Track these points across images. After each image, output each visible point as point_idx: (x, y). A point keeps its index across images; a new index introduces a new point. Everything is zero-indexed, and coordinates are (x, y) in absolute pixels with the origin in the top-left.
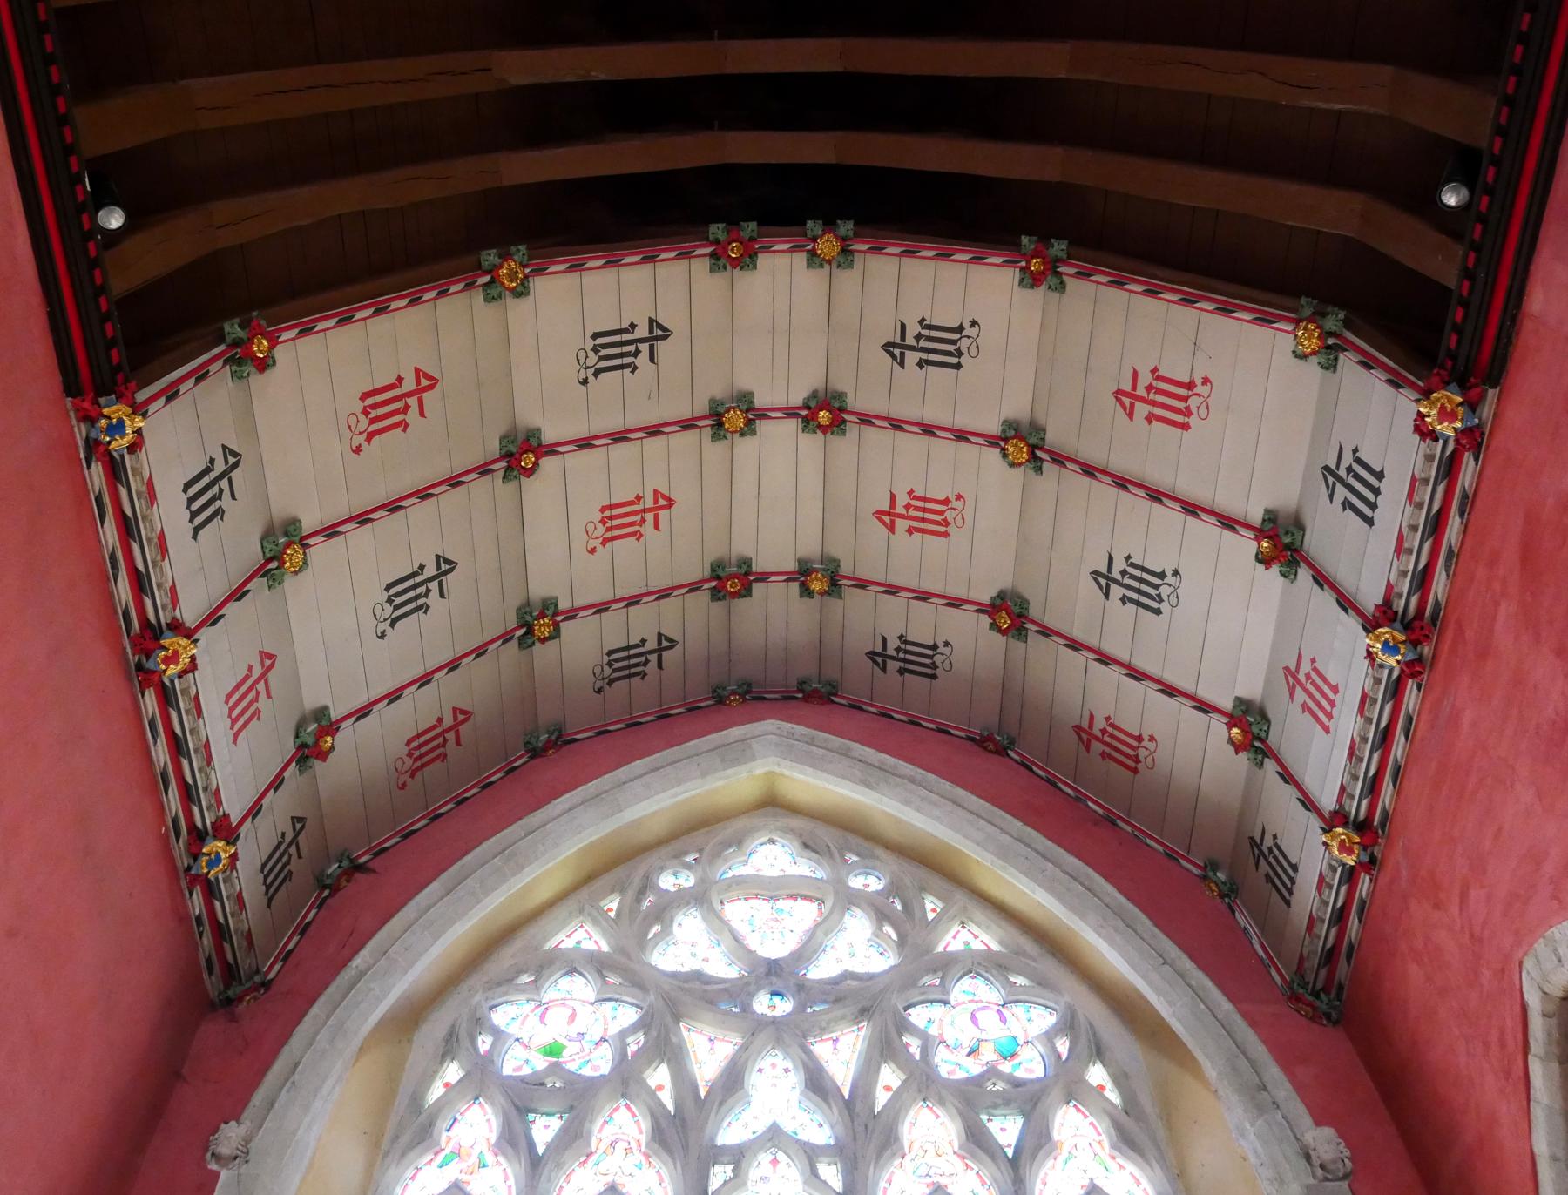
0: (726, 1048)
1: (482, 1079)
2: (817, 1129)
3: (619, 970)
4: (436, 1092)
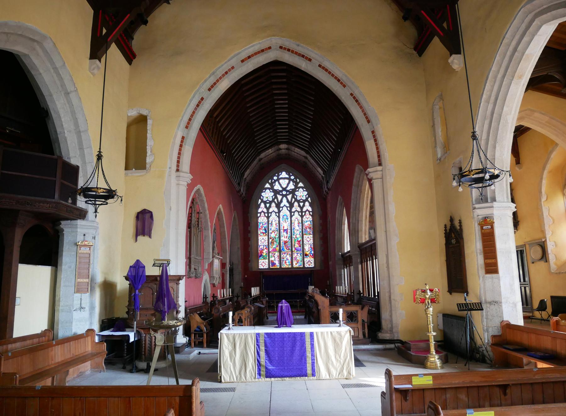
0: (281, 197)
1: (262, 201)
2: (288, 205)
3: (272, 188)
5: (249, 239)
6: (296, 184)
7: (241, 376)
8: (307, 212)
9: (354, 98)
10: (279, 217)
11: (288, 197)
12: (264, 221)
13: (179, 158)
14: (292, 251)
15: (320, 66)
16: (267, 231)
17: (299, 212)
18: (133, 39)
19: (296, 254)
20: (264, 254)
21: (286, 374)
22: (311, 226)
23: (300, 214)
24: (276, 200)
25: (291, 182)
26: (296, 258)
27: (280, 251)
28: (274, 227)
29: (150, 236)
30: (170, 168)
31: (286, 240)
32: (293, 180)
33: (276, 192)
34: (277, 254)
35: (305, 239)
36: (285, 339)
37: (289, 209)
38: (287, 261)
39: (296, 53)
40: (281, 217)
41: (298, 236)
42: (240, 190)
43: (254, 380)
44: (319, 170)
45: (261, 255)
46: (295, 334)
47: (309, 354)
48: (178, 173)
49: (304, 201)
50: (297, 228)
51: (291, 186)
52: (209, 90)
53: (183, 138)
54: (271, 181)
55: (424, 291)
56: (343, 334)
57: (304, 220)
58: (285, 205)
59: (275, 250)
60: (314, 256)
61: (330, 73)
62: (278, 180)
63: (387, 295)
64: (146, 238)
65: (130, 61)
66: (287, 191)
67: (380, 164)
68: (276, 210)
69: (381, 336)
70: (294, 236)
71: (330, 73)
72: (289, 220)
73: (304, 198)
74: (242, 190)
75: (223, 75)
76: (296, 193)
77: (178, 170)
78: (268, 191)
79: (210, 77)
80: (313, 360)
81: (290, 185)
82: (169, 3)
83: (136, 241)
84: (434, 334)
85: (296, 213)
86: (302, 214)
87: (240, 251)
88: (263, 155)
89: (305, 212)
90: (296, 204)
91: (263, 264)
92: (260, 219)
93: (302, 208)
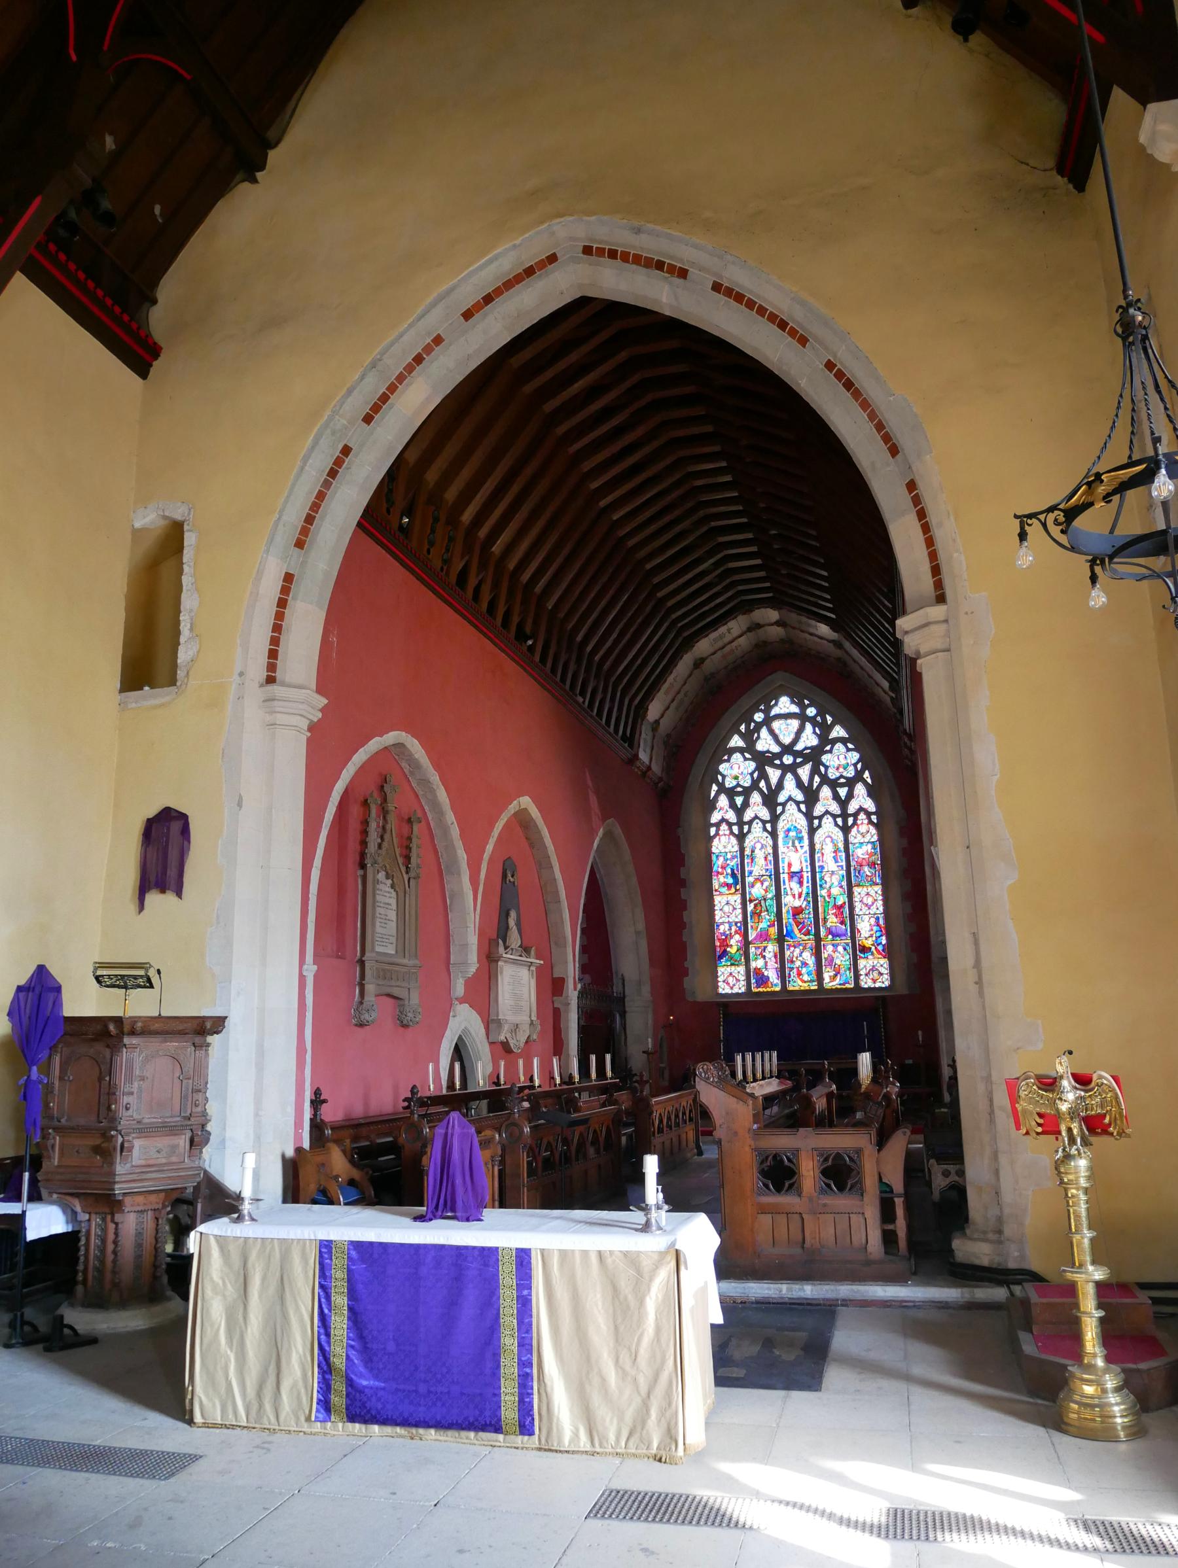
0: (778, 773)
1: (722, 789)
2: (800, 797)
3: (750, 748)
4: (713, 794)
5: (683, 906)
6: (824, 731)
7: (261, 1406)
8: (862, 816)
9: (840, 375)
10: (774, 834)
11: (800, 771)
12: (729, 848)
13: (275, 641)
14: (818, 939)
15: (717, 287)
16: (739, 879)
17: (834, 817)
18: (154, 302)
19: (830, 948)
20: (733, 950)
21: (421, 1413)
22: (877, 859)
23: (839, 821)
24: (762, 784)
25: (809, 727)
26: (831, 960)
27: (781, 940)
28: (759, 866)
29: (179, 893)
30: (241, 674)
31: (797, 903)
32: (812, 720)
33: (763, 760)
34: (772, 948)
35: (857, 899)
36: (424, 1271)
37: (803, 807)
38: (804, 970)
39: (637, 260)
40: (781, 835)
41: (835, 891)
42: (636, 756)
43: (306, 1427)
44: (878, 677)
45: (724, 953)
46: (460, 1252)
47: (509, 1341)
48: (270, 688)
49: (851, 783)
50: (831, 865)
51: (809, 739)
52: (368, 419)
53: (289, 578)
54: (747, 727)
55: (1049, 1084)
56: (646, 1264)
57: (851, 839)
58: (790, 799)
59: (764, 936)
60: (889, 952)
61: (750, 304)
62: (768, 721)
63: (981, 1088)
64: (170, 898)
65: (142, 368)
66: (796, 754)
67: (941, 599)
68: (765, 814)
69: (972, 1249)
70: (824, 893)
71: (750, 304)
72: (806, 842)
73: (851, 773)
74: (643, 756)
75: (410, 369)
76: (825, 758)
77: (271, 680)
78: (737, 757)
79: (362, 378)
80: (525, 1365)
81: (804, 735)
82: (254, 181)
83: (141, 907)
84: (1099, 1274)
85: (828, 822)
86: (845, 821)
87: (644, 944)
88: (703, 646)
89: (855, 815)
90: (826, 792)
91: (731, 980)
92: (716, 842)
93: (843, 803)
